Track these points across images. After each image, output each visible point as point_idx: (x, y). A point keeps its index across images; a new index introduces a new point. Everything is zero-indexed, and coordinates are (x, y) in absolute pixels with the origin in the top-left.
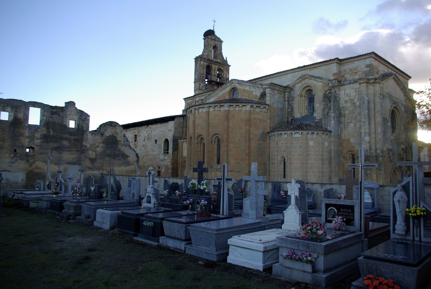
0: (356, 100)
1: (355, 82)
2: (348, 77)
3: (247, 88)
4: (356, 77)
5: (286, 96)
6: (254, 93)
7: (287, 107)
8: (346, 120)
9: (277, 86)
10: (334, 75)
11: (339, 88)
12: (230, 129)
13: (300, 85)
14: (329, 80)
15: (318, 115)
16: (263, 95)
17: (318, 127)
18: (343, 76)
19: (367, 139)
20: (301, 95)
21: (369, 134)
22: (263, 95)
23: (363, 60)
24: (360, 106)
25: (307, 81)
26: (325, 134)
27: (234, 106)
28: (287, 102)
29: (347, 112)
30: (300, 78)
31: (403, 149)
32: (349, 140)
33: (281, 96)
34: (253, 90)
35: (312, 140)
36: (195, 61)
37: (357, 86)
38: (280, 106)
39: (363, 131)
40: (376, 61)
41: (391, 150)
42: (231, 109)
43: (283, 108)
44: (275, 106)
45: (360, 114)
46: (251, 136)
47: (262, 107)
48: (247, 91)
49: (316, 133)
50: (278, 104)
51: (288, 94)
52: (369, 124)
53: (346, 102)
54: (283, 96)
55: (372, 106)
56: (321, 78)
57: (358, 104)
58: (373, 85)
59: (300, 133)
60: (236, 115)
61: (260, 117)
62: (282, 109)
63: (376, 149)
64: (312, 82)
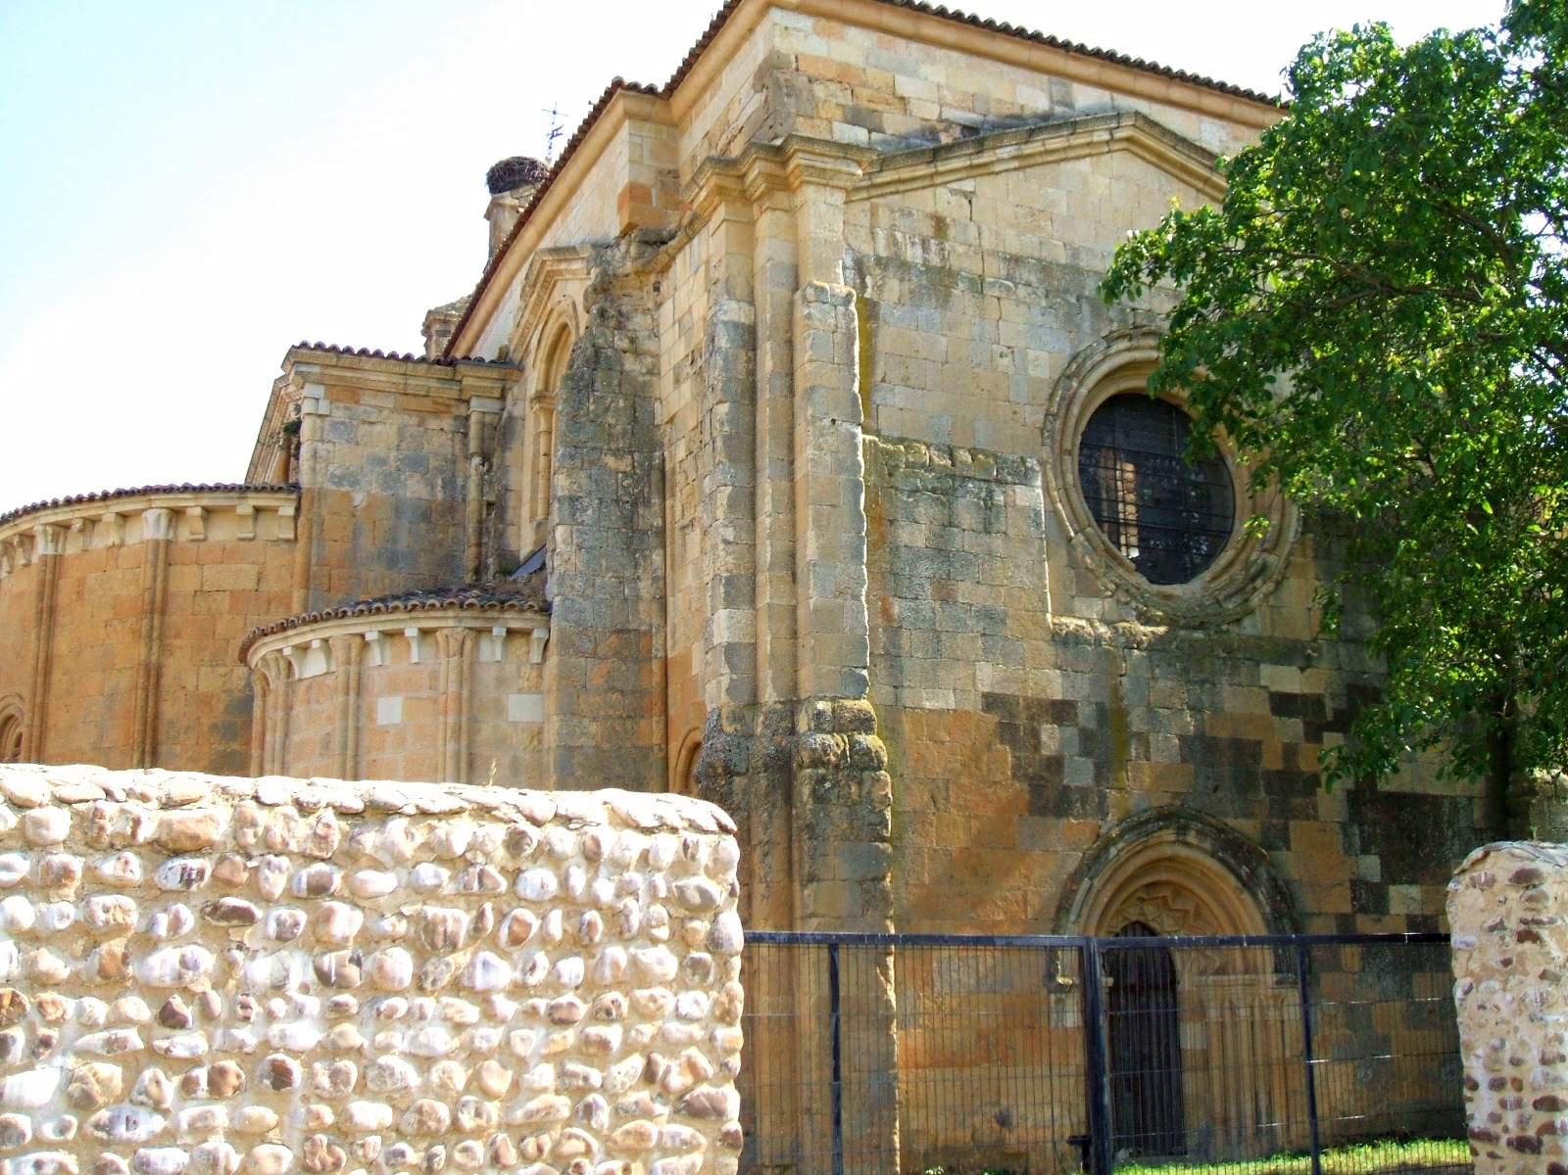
5: (474, 419)
7: (473, 492)
8: (678, 513)
9: (367, 364)
11: (657, 289)
12: (57, 676)
19: (724, 626)
20: (539, 397)
21: (741, 589)
23: (746, 46)
26: (499, 631)
27: (77, 525)
28: (476, 460)
29: (681, 452)
31: (1283, 704)
32: (686, 661)
33: (433, 424)
35: (393, 688)
38: (414, 488)
40: (853, 32)
41: (1061, 712)
42: (72, 547)
43: (451, 508)
44: (359, 498)
46: (169, 710)
47: (245, 507)
49: (411, 632)
50: (390, 480)
51: (495, 406)
52: (746, 503)
54: (447, 423)
55: (768, 362)
58: (781, 198)
59: (316, 644)
60: (92, 579)
61: (242, 576)
62: (442, 513)
63: (792, 704)
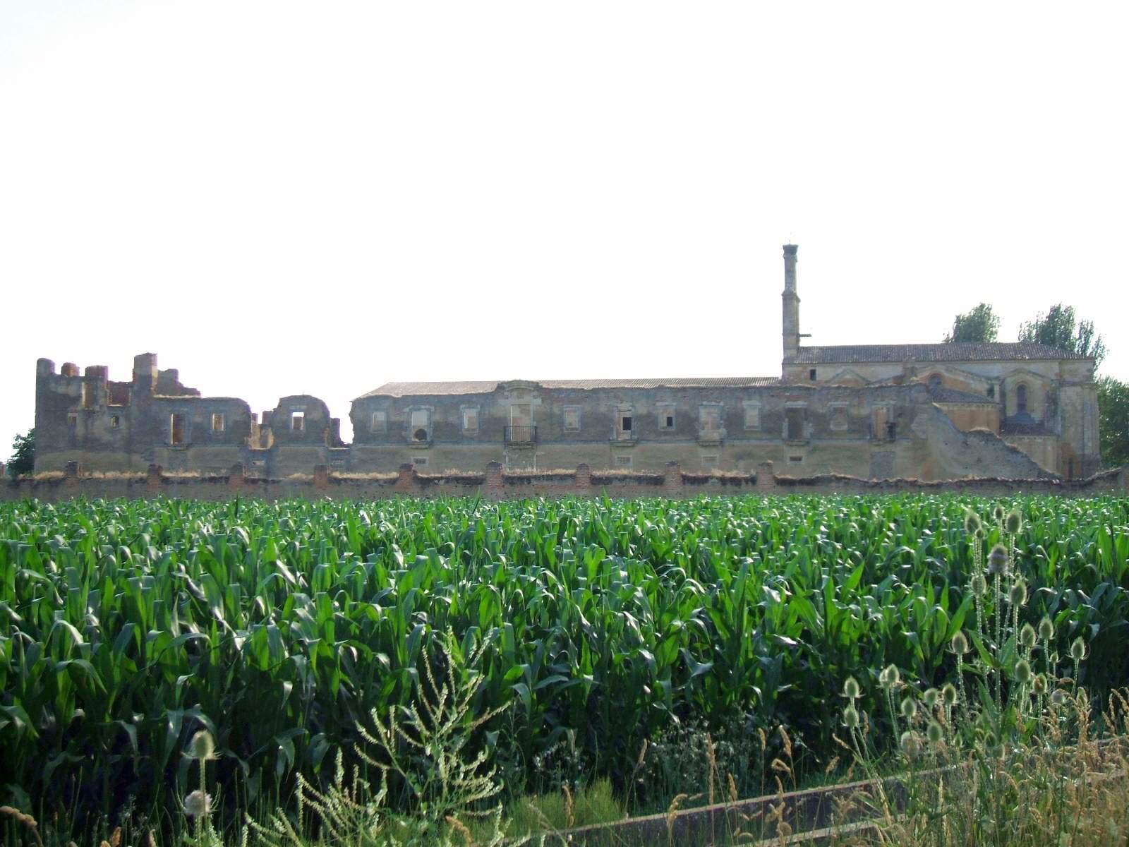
0: (1077, 404)
1: (1074, 384)
2: (1067, 377)
3: (961, 379)
4: (1076, 380)
6: (973, 386)
10: (1056, 374)
13: (1013, 379)
14: (1052, 380)
15: (1037, 416)
16: (991, 391)
17: (1039, 429)
18: (1061, 376)
22: (991, 391)
24: (1082, 410)
25: (1021, 375)
30: (1015, 371)
34: (972, 382)
36: (784, 300)
37: (1078, 389)
39: (1086, 436)
45: (1083, 418)
48: (961, 382)
53: (1066, 405)
56: (1042, 376)
57: (1079, 408)
64: (1029, 378)
